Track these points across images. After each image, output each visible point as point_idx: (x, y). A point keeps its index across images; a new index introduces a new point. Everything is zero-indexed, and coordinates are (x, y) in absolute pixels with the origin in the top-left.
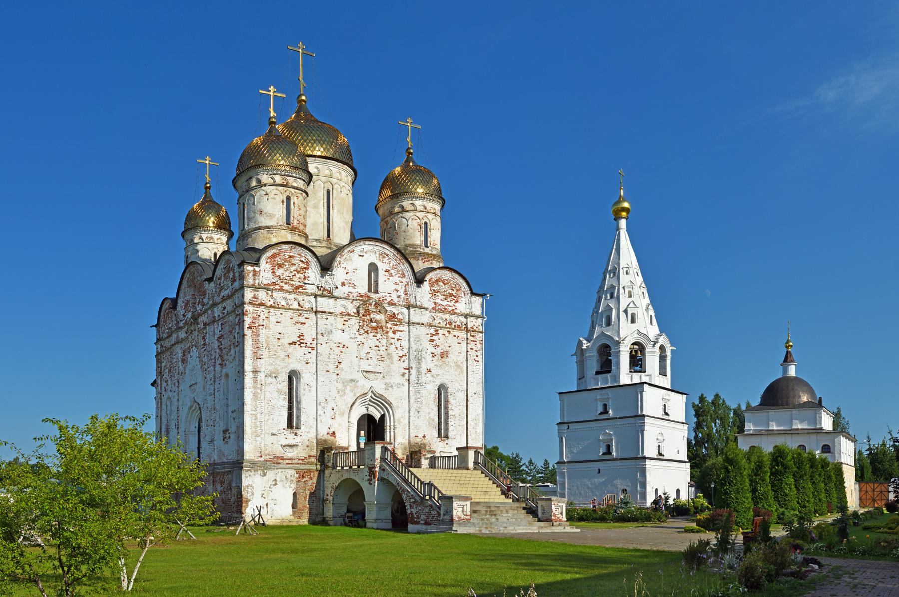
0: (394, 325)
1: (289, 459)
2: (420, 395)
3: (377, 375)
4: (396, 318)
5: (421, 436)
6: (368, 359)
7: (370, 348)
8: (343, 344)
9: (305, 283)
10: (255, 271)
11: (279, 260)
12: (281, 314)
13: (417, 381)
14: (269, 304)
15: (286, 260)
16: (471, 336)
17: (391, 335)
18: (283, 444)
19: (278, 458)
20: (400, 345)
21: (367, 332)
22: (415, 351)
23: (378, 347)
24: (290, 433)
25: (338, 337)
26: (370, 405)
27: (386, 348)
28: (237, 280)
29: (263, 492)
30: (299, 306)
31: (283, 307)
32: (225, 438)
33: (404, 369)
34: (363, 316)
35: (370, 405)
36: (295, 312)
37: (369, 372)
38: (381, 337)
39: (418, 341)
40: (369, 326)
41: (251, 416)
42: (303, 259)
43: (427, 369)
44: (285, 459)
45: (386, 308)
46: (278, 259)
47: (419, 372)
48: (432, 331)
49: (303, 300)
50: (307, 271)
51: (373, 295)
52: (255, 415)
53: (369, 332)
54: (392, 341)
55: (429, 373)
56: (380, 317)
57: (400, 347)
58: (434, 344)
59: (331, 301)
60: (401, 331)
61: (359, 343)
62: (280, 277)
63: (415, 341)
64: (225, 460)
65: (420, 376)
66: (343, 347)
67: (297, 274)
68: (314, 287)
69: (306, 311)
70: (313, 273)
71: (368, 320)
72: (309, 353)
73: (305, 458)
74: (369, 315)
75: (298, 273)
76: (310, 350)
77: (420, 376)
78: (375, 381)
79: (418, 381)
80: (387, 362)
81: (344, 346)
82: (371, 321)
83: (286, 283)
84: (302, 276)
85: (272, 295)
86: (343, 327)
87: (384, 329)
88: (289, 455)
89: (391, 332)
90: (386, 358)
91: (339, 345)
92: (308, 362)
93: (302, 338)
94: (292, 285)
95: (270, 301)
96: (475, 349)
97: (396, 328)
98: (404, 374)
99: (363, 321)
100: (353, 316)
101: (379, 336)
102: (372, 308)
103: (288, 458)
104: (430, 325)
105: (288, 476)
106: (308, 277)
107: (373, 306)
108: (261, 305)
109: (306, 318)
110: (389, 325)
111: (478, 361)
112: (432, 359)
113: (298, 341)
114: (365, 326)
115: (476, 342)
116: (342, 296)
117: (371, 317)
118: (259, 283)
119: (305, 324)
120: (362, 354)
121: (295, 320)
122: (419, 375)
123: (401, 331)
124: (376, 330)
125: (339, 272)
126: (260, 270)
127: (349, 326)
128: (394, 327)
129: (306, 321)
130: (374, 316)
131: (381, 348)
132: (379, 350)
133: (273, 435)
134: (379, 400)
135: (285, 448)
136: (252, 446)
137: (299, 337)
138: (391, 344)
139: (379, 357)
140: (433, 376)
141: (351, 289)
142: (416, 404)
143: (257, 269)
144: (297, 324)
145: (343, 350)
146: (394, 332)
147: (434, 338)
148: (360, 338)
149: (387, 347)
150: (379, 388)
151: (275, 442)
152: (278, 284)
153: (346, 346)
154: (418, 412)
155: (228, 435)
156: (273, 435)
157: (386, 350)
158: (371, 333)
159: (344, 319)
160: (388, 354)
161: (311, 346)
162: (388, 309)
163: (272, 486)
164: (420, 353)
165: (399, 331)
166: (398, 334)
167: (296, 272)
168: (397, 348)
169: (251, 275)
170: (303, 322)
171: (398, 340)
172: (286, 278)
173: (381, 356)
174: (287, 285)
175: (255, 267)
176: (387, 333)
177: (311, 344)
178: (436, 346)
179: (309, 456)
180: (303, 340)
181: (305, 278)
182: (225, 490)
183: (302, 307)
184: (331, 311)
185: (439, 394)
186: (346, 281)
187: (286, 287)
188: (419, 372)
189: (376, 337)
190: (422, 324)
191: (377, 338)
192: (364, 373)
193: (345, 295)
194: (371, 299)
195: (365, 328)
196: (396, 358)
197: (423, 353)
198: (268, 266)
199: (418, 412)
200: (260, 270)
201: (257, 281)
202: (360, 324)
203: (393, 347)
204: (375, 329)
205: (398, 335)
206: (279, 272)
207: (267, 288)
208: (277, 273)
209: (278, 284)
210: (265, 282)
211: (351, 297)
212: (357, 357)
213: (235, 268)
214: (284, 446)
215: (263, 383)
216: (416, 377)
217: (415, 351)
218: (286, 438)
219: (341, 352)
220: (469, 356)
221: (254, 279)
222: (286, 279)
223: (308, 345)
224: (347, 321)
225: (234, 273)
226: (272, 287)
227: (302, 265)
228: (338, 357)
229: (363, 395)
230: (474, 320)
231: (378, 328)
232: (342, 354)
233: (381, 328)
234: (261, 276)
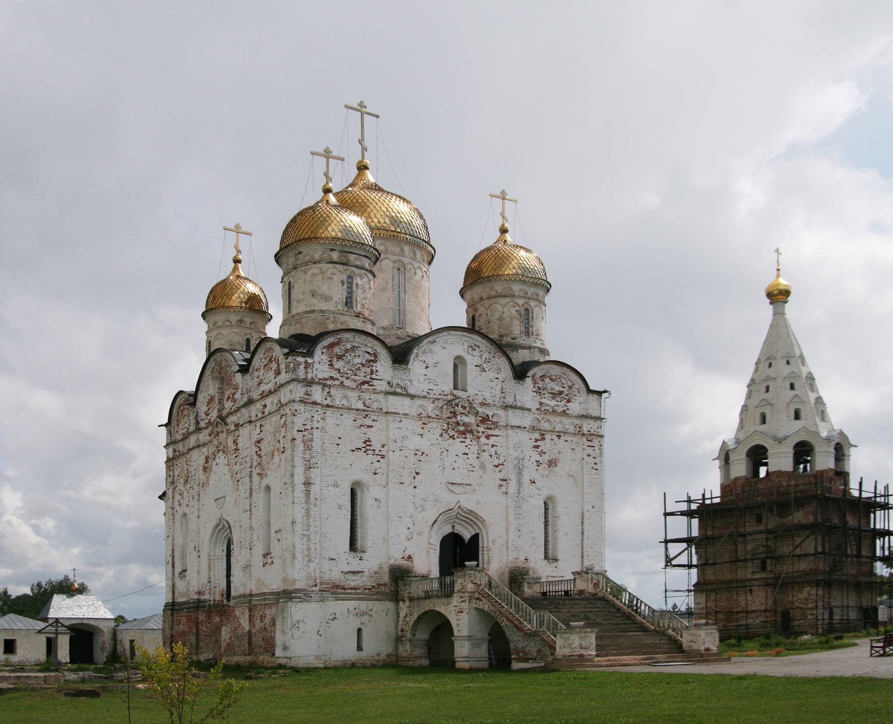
1: (352, 589)
3: (466, 487)
4: (490, 421)
5: (522, 558)
7: (457, 455)
8: (422, 451)
9: (373, 379)
10: (308, 363)
11: (339, 350)
12: (341, 415)
14: (325, 402)
15: (347, 351)
16: (587, 440)
17: (483, 440)
18: (345, 570)
19: (337, 587)
21: (452, 437)
22: (515, 459)
23: (467, 454)
24: (354, 557)
25: (415, 442)
26: (456, 523)
27: (478, 456)
28: (283, 373)
30: (365, 406)
31: (343, 406)
32: (266, 563)
33: (501, 480)
35: (456, 523)
36: (359, 412)
37: (455, 484)
38: (471, 443)
40: (456, 430)
41: (302, 537)
42: (369, 350)
43: (531, 480)
45: (477, 408)
46: (337, 350)
47: (520, 483)
48: (537, 435)
49: (370, 399)
50: (374, 364)
51: (459, 393)
52: (308, 537)
53: (455, 437)
54: (485, 447)
55: (533, 484)
56: (470, 419)
58: (539, 450)
59: (406, 401)
62: (339, 370)
64: (266, 591)
65: (521, 488)
67: (361, 368)
68: (385, 384)
69: (373, 412)
70: (384, 367)
71: (455, 423)
73: (373, 587)
75: (363, 366)
78: (464, 496)
81: (423, 453)
83: (347, 378)
84: (369, 370)
85: (329, 392)
86: (421, 432)
87: (475, 433)
88: (353, 584)
89: (483, 436)
90: (477, 467)
91: (417, 452)
94: (355, 381)
95: (326, 399)
96: (593, 455)
97: (490, 432)
98: (501, 486)
99: (448, 424)
100: (434, 418)
101: (468, 441)
102: (459, 409)
103: (351, 587)
104: (533, 429)
106: (377, 371)
107: (460, 406)
108: (315, 403)
109: (374, 420)
110: (481, 429)
111: (597, 470)
112: (538, 467)
114: (450, 430)
115: (594, 447)
116: (420, 395)
117: (458, 420)
118: (312, 377)
119: (372, 427)
121: (360, 422)
124: (465, 434)
125: (415, 365)
126: (314, 362)
128: (487, 431)
129: (373, 424)
130: (462, 418)
132: (468, 458)
133: (333, 559)
134: (470, 517)
135: (347, 576)
136: (305, 573)
138: (484, 451)
141: (431, 386)
143: (310, 360)
144: (362, 428)
145: (423, 458)
146: (488, 437)
147: (538, 443)
148: (444, 444)
149: (478, 454)
150: (468, 502)
152: (338, 379)
153: (426, 453)
155: (269, 561)
156: (333, 559)
157: (478, 458)
158: (458, 437)
161: (380, 453)
162: (480, 410)
164: (521, 461)
165: (494, 435)
166: (493, 439)
167: (361, 366)
168: (491, 456)
169: (302, 367)
170: (370, 424)
171: (493, 446)
172: (348, 372)
174: (349, 381)
175: (306, 358)
176: (478, 438)
177: (380, 451)
178: (542, 453)
179: (378, 584)
180: (370, 446)
181: (372, 373)
182: (266, 627)
183: (368, 407)
184: (406, 412)
185: (546, 509)
187: (347, 383)
188: (520, 483)
189: (464, 442)
190: (525, 428)
191: (466, 444)
194: (458, 398)
195: (450, 433)
197: (526, 461)
198: (325, 358)
200: (314, 362)
201: (310, 376)
202: (444, 428)
203: (486, 454)
204: (463, 433)
205: (492, 440)
206: (338, 364)
207: (323, 384)
208: (336, 366)
209: (338, 379)
210: (320, 376)
211: (432, 396)
213: (280, 359)
214: (346, 573)
215: (318, 497)
217: (515, 459)
219: (420, 461)
220: (585, 463)
221: (306, 372)
222: (347, 374)
225: (278, 364)
226: (329, 382)
227: (368, 357)
228: (415, 466)
229: (448, 511)
230: (591, 422)
231: (467, 431)
233: (471, 432)
234: (314, 369)
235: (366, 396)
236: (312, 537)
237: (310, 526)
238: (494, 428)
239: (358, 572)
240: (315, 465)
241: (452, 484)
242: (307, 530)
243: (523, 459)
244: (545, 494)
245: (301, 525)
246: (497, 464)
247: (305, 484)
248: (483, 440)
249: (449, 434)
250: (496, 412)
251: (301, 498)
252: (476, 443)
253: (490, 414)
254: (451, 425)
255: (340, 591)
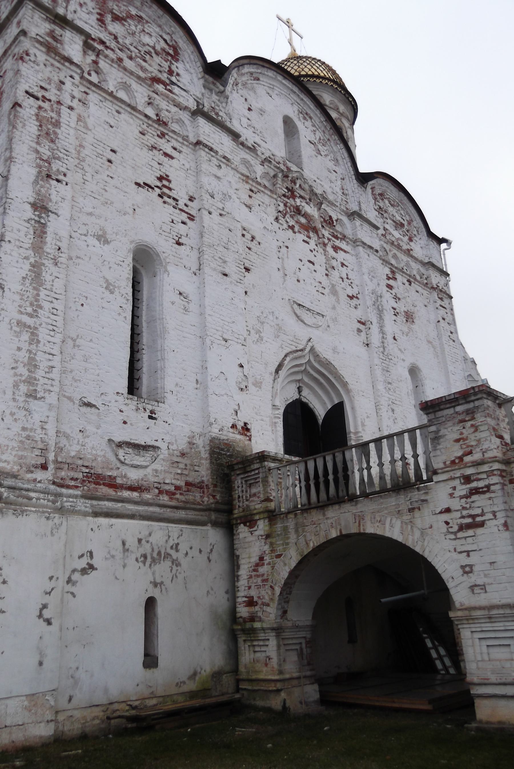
1: (132, 488)
18: (118, 439)
24: (137, 409)
29: (46, 599)
44: (121, 487)
52: (34, 333)
60: (345, 252)
72: (183, 223)
73: (177, 488)
76: (184, 217)
92: (180, 241)
93: (165, 183)
103: (129, 483)
105: (132, 543)
113: (157, 187)
123: (345, 252)
127: (261, 204)
133: (89, 405)
135: (121, 453)
137: (160, 179)
151: (90, 429)
153: (258, 238)
156: (89, 405)
163: (76, 576)
179: (188, 484)
192: (295, 306)
214: (120, 445)
218: (125, 423)
223: (181, 205)
235: (158, 100)
236: (43, 334)
237: (41, 307)
239: (146, 448)
240: (61, 177)
241: (299, 305)
242: (31, 316)
245: (17, 297)
247: (34, 206)
250: (340, 217)
251: (22, 234)
253: (334, 218)
255: (104, 490)
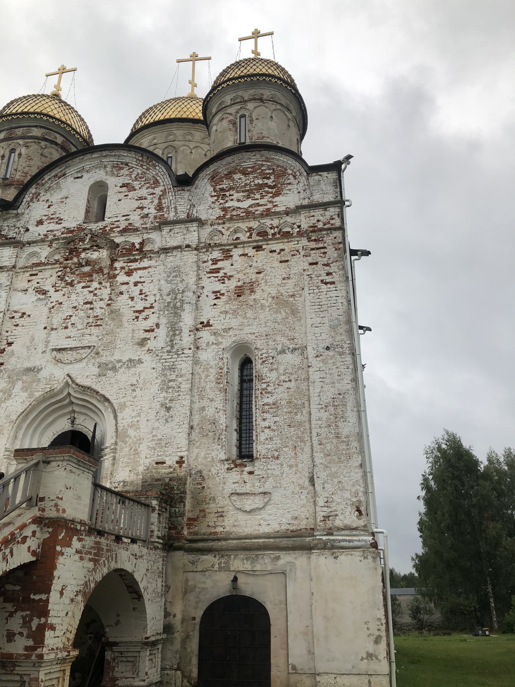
0: (130, 262)
2: (176, 373)
6: (66, 328)
7: (75, 307)
13: (169, 348)
20: (141, 290)
21: (71, 284)
23: (91, 303)
33: (146, 331)
34: (66, 260)
37: (64, 349)
39: (176, 276)
40: (77, 273)
53: (76, 282)
54: (124, 288)
55: (208, 328)
57: (141, 294)
60: (145, 268)
61: (53, 304)
63: (168, 276)
66: (22, 317)
71: (75, 264)
74: (78, 256)
77: (178, 338)
78: (77, 366)
79: (172, 346)
80: (109, 324)
82: (80, 265)
97: (134, 265)
101: (95, 285)
112: (216, 301)
120: (57, 320)
122: (174, 335)
123: (145, 268)
124: (92, 276)
128: (129, 264)
131: (98, 305)
138: (121, 293)
139: (91, 320)
140: (215, 334)
142: (165, 394)
145: (21, 322)
146: (129, 273)
148: (55, 296)
149: (110, 299)
153: (27, 313)
154: (168, 409)
158: (79, 282)
159: (31, 273)
160: (112, 312)
164: (179, 296)
168: (132, 299)
171: (136, 284)
173: (97, 316)
186: (45, 218)
189: (89, 287)
190: (188, 246)
191: (90, 289)
193: (43, 237)
196: (128, 315)
199: (168, 409)
203: (125, 296)
205: (136, 277)
212: (45, 328)
216: (168, 340)
224: (37, 275)
232: (18, 327)
238: (141, 259)
243: (183, 291)
244: (227, 342)
246: (142, 309)
248: (122, 278)
249: (66, 281)
252: (108, 285)
254: (70, 268)
